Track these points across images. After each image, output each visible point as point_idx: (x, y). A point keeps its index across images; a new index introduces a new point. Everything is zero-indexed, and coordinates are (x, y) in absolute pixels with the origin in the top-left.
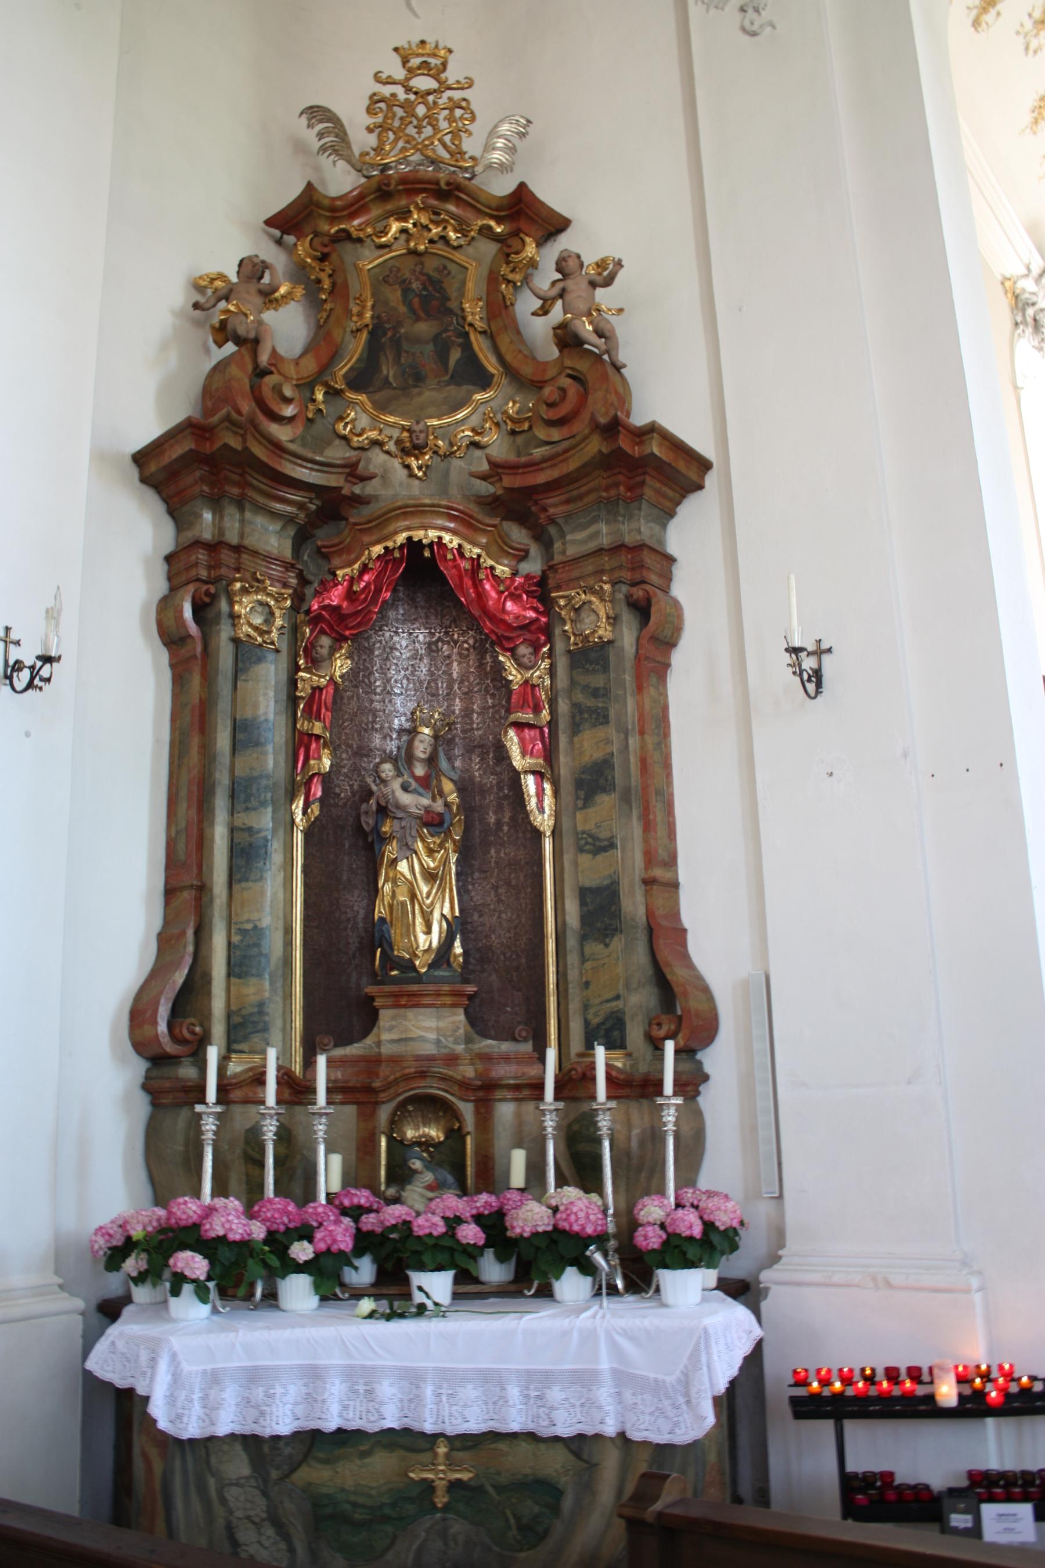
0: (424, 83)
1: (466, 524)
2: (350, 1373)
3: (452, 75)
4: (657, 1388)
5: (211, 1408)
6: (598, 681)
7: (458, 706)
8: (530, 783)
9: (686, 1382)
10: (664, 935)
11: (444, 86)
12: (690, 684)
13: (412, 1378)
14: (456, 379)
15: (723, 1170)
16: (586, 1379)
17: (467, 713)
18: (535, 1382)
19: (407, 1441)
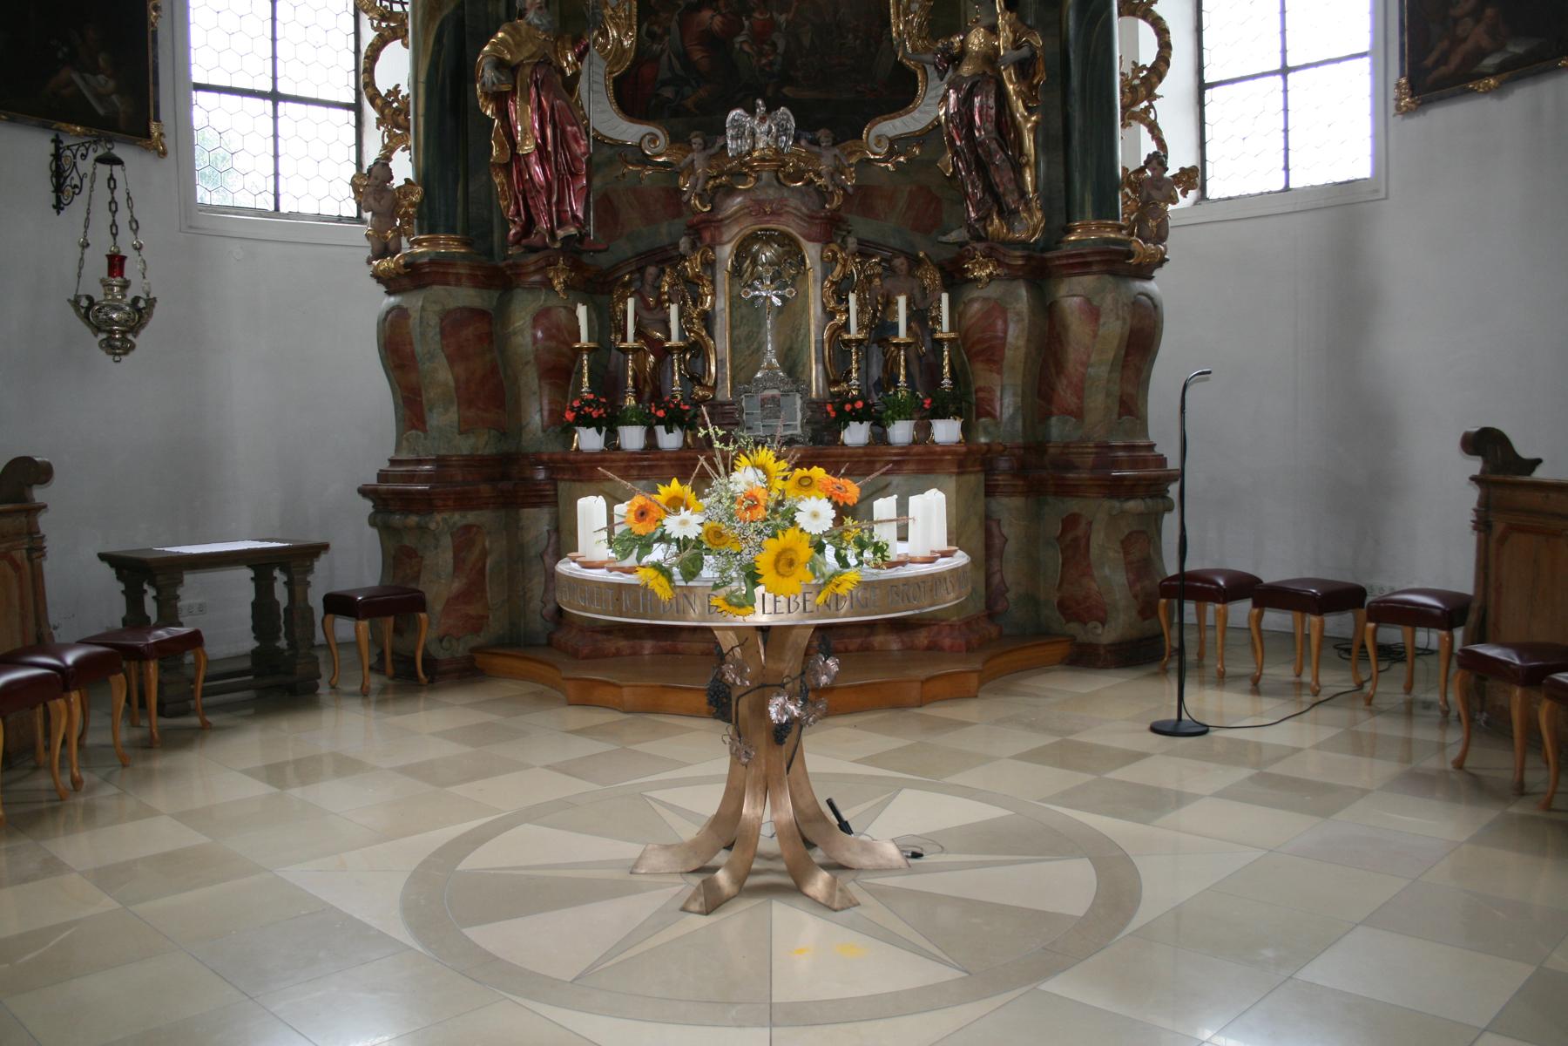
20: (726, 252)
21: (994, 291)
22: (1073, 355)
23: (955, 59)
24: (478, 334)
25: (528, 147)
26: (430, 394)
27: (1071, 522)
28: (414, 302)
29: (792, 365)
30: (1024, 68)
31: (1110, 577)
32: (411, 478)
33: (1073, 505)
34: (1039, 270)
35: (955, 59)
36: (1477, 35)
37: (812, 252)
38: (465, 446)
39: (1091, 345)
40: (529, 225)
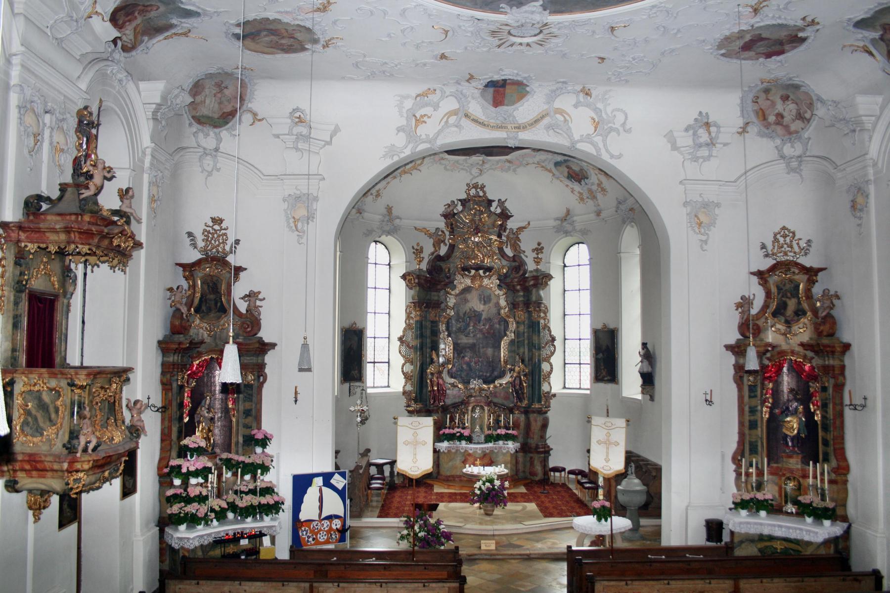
0: (217, 227)
3: (224, 225)
6: (250, 392)
11: (221, 229)
14: (219, 311)
20: (470, 408)
22: (532, 428)
27: (531, 458)
30: (525, 375)
31: (538, 468)
33: (531, 455)
34: (527, 412)
36: (604, 373)
37: (486, 408)
39: (536, 426)
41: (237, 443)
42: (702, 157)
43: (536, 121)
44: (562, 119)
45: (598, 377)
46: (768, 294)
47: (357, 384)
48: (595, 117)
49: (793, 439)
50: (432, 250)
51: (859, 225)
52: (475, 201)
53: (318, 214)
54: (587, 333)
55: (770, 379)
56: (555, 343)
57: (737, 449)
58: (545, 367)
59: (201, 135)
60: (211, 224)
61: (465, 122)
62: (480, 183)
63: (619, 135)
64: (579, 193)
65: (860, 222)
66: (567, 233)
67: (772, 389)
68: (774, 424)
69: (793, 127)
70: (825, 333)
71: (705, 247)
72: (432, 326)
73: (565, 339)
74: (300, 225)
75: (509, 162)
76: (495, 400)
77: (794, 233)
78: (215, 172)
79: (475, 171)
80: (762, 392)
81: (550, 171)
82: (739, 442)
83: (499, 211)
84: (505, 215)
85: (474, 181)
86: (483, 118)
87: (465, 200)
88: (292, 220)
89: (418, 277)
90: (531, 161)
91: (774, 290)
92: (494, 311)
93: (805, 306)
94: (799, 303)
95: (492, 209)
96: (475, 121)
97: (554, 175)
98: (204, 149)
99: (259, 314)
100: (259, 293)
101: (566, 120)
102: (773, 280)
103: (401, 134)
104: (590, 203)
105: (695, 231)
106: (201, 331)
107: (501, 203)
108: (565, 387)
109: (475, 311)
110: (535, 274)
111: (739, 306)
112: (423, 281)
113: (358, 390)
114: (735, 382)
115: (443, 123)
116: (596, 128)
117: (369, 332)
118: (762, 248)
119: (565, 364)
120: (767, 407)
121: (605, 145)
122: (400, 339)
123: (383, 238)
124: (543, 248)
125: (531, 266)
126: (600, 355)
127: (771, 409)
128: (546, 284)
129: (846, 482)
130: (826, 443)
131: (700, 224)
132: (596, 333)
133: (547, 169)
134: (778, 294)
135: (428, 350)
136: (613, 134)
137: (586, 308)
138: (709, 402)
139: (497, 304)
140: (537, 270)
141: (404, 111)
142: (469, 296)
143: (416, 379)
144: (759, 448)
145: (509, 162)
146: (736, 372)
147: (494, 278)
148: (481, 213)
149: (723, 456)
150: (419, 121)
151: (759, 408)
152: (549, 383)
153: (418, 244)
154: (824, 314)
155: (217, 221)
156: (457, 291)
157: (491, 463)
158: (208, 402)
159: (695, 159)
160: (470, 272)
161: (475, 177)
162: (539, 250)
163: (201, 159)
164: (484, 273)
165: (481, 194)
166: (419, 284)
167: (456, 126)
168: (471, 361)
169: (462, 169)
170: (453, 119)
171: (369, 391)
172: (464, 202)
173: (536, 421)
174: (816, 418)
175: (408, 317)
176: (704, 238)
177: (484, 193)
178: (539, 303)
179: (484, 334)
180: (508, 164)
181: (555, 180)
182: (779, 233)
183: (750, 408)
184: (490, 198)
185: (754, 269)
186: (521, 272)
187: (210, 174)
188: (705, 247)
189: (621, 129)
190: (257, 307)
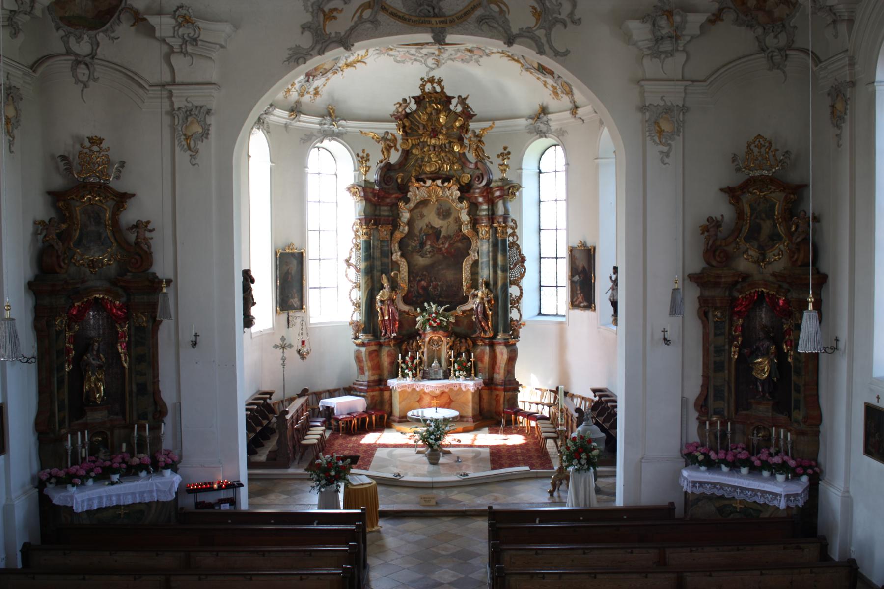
0: (95, 148)
1: (107, 292)
2: (107, 497)
4: (164, 492)
5: (82, 507)
7: (101, 332)
8: (122, 355)
9: (170, 490)
10: (156, 393)
12: (164, 334)
13: (119, 496)
15: (167, 443)
16: (151, 492)
17: (104, 333)
18: (142, 493)
19: (118, 507)
21: (482, 348)
23: (475, 296)
24: (375, 355)
25: (386, 318)
26: (366, 368)
28: (363, 349)
29: (440, 362)
30: (489, 302)
32: (362, 385)
33: (498, 392)
35: (475, 296)
36: (580, 299)
38: (372, 378)
40: (386, 332)
41: (131, 392)
42: (665, 52)
43: (466, 14)
44: (497, 9)
45: (574, 304)
46: (740, 214)
47: (298, 314)
48: (536, 6)
49: (763, 382)
50: (382, 157)
51: (837, 135)
52: (433, 99)
53: (213, 131)
54: (563, 252)
55: (740, 314)
56: (525, 264)
57: (701, 394)
58: (513, 291)
59: (72, 40)
60: (87, 143)
61: (383, 17)
62: (436, 77)
63: (565, 27)
64: (553, 87)
65: (838, 132)
66: (542, 134)
67: (742, 326)
68: (744, 365)
69: (777, 13)
70: (799, 263)
71: (667, 160)
72: (382, 246)
73: (541, 258)
74: (192, 143)
75: (470, 51)
76: (457, 330)
77: (770, 143)
78: (91, 83)
79: (430, 62)
80: (730, 330)
81: (517, 61)
82: (702, 386)
83: (459, 109)
84: (468, 115)
85: (431, 75)
86: (404, 10)
87: (419, 97)
88: (183, 137)
89: (364, 189)
90: (495, 50)
91: (747, 209)
92: (454, 227)
93: (781, 229)
94: (775, 226)
95: (452, 107)
96: (394, 15)
97: (523, 65)
98: (77, 55)
99: (149, 247)
100: (148, 222)
101: (502, 12)
102: (746, 199)
103: (308, 34)
104: (566, 100)
105: (654, 141)
106: (83, 268)
107: (462, 101)
108: (540, 314)
109: (432, 227)
110: (500, 184)
111: (705, 229)
112: (370, 195)
113: (298, 321)
114: (700, 317)
115: (355, 18)
116: (538, 20)
117: (311, 254)
118: (734, 161)
119: (541, 286)
120: (736, 347)
121: (549, 41)
122: (347, 261)
123: (326, 143)
124: (509, 153)
125: (496, 175)
126: (576, 278)
127: (741, 347)
128: (514, 194)
129: (817, 434)
130: (798, 390)
131: (661, 132)
132: (572, 251)
133: (514, 59)
134: (751, 215)
135: (379, 274)
136: (559, 26)
137: (563, 224)
138: (667, 341)
139: (458, 221)
140: (503, 179)
141: (309, 4)
142: (425, 211)
143: (363, 307)
144: (726, 394)
145: (470, 51)
146: (701, 307)
147: (455, 187)
148: (438, 112)
149: (684, 402)
150: (330, 16)
151: (727, 347)
152: (519, 310)
153: (363, 151)
154: (798, 240)
155: (95, 141)
156: (411, 205)
157: (448, 405)
158: (96, 348)
159: (655, 53)
160: (425, 182)
161: (433, 69)
162: (505, 154)
163: (73, 69)
164: (443, 183)
165: (438, 89)
166: (366, 198)
167: (372, 22)
168: (429, 285)
169: (416, 60)
170: (367, 14)
171: (312, 321)
172: (418, 100)
173: (502, 354)
174: (789, 360)
175: (357, 236)
176: (665, 149)
177: (442, 88)
178: (506, 217)
179: (443, 254)
180: (468, 54)
181: (524, 72)
182: (754, 142)
183: (715, 347)
184: (449, 94)
185: (724, 186)
186: (484, 183)
187: (86, 86)
188: (667, 160)
189: (568, 20)
190: (145, 239)
